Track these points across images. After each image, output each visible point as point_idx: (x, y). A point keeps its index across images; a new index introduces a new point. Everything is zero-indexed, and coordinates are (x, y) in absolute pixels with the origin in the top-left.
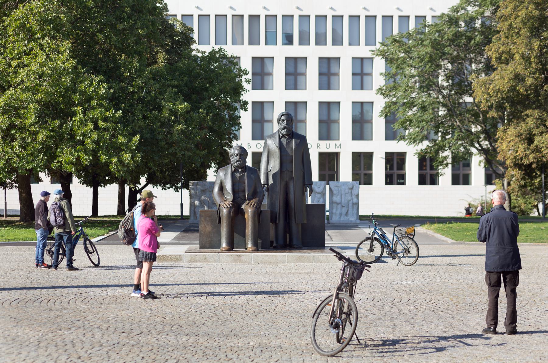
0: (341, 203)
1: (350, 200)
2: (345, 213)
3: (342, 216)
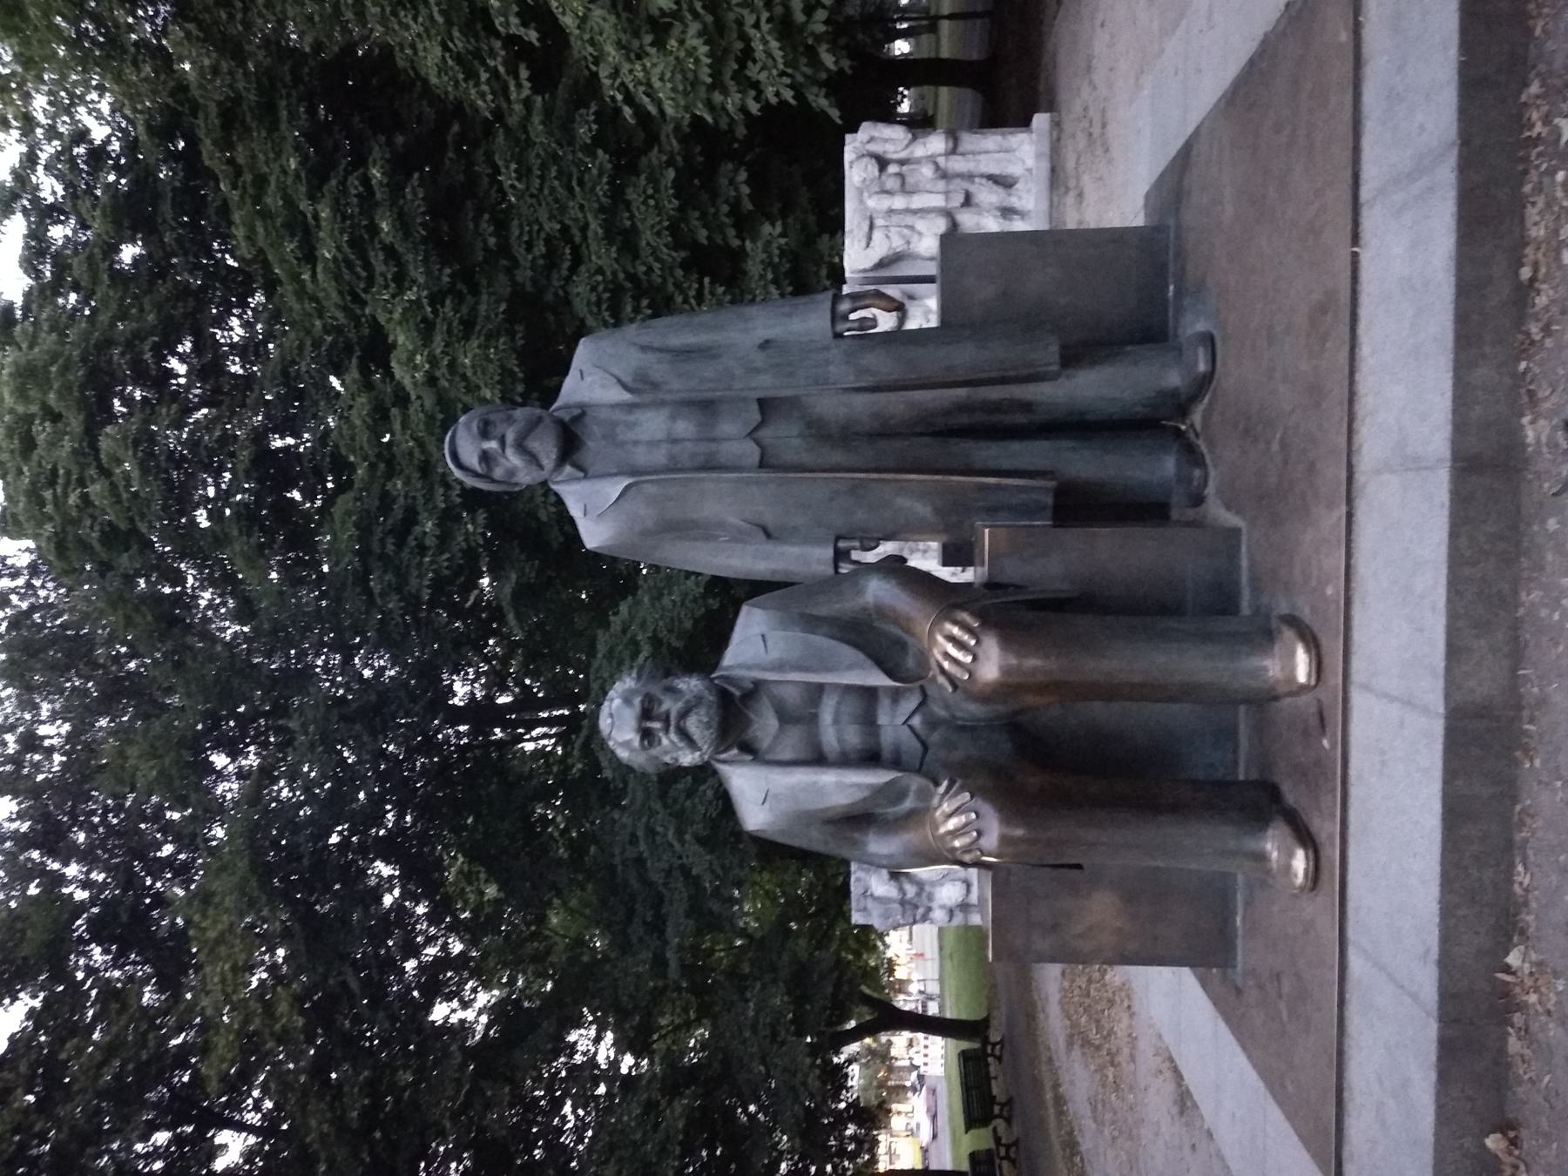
0: (948, 214)
1: (936, 165)
2: (1000, 190)
3: (1014, 202)
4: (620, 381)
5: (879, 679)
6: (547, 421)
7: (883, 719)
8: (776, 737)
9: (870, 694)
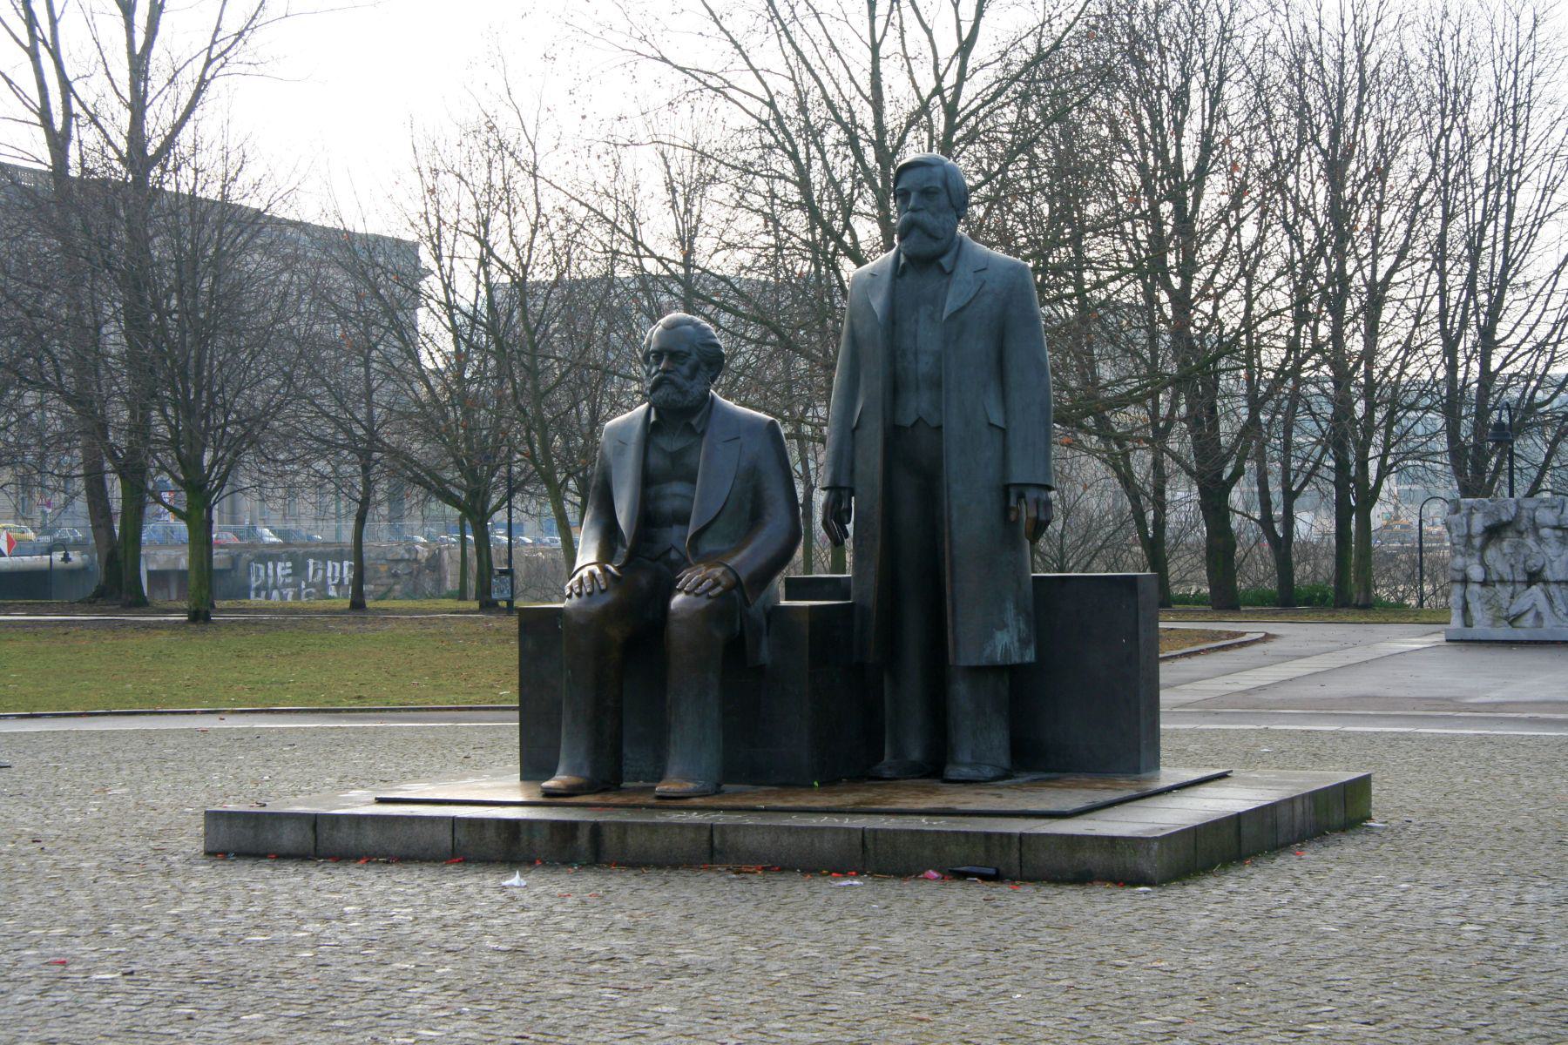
4: (961, 309)
5: (692, 529)
6: (935, 247)
7: (676, 530)
8: (663, 451)
9: (683, 519)
